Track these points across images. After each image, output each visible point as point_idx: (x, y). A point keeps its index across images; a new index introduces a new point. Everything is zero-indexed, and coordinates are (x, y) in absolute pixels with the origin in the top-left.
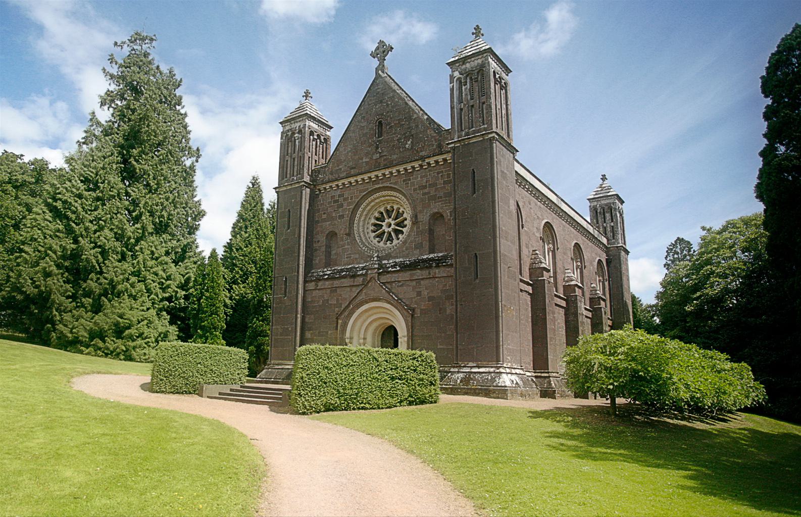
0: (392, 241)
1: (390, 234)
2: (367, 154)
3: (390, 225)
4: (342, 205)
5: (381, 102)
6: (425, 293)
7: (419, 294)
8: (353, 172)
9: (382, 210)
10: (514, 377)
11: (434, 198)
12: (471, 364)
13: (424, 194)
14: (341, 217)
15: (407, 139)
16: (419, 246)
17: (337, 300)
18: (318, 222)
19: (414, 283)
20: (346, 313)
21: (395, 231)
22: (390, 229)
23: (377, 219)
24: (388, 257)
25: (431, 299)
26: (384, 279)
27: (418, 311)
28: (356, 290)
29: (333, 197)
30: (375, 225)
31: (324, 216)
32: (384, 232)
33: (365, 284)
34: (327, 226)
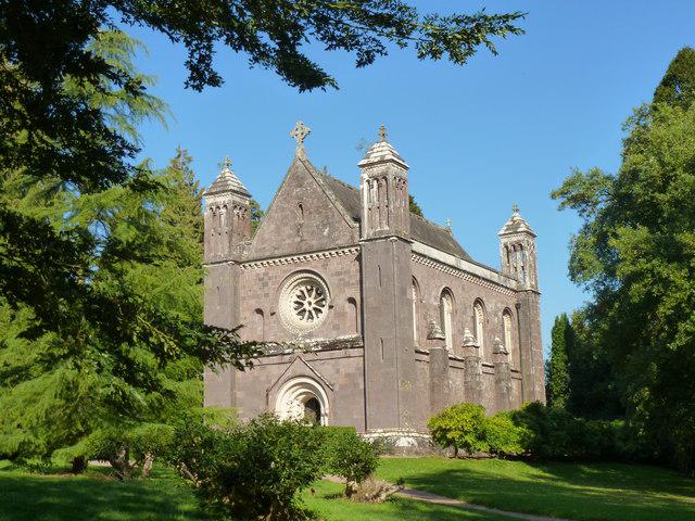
0: (312, 318)
1: (310, 312)
2: (290, 236)
3: (310, 303)
4: (265, 285)
5: (301, 186)
6: (342, 370)
7: (338, 371)
8: (277, 253)
9: (303, 288)
10: (410, 440)
11: (348, 284)
12: (379, 431)
13: (340, 280)
14: (267, 295)
15: (325, 226)
16: (336, 327)
17: (267, 376)
18: (244, 298)
19: (333, 361)
20: (276, 388)
21: (315, 309)
22: (311, 308)
23: (298, 297)
24: (310, 335)
25: (347, 375)
26: (310, 356)
27: (336, 388)
28: (285, 367)
29: (258, 275)
30: (296, 302)
31: (250, 294)
32: (304, 310)
33: (291, 362)
34: (254, 304)
